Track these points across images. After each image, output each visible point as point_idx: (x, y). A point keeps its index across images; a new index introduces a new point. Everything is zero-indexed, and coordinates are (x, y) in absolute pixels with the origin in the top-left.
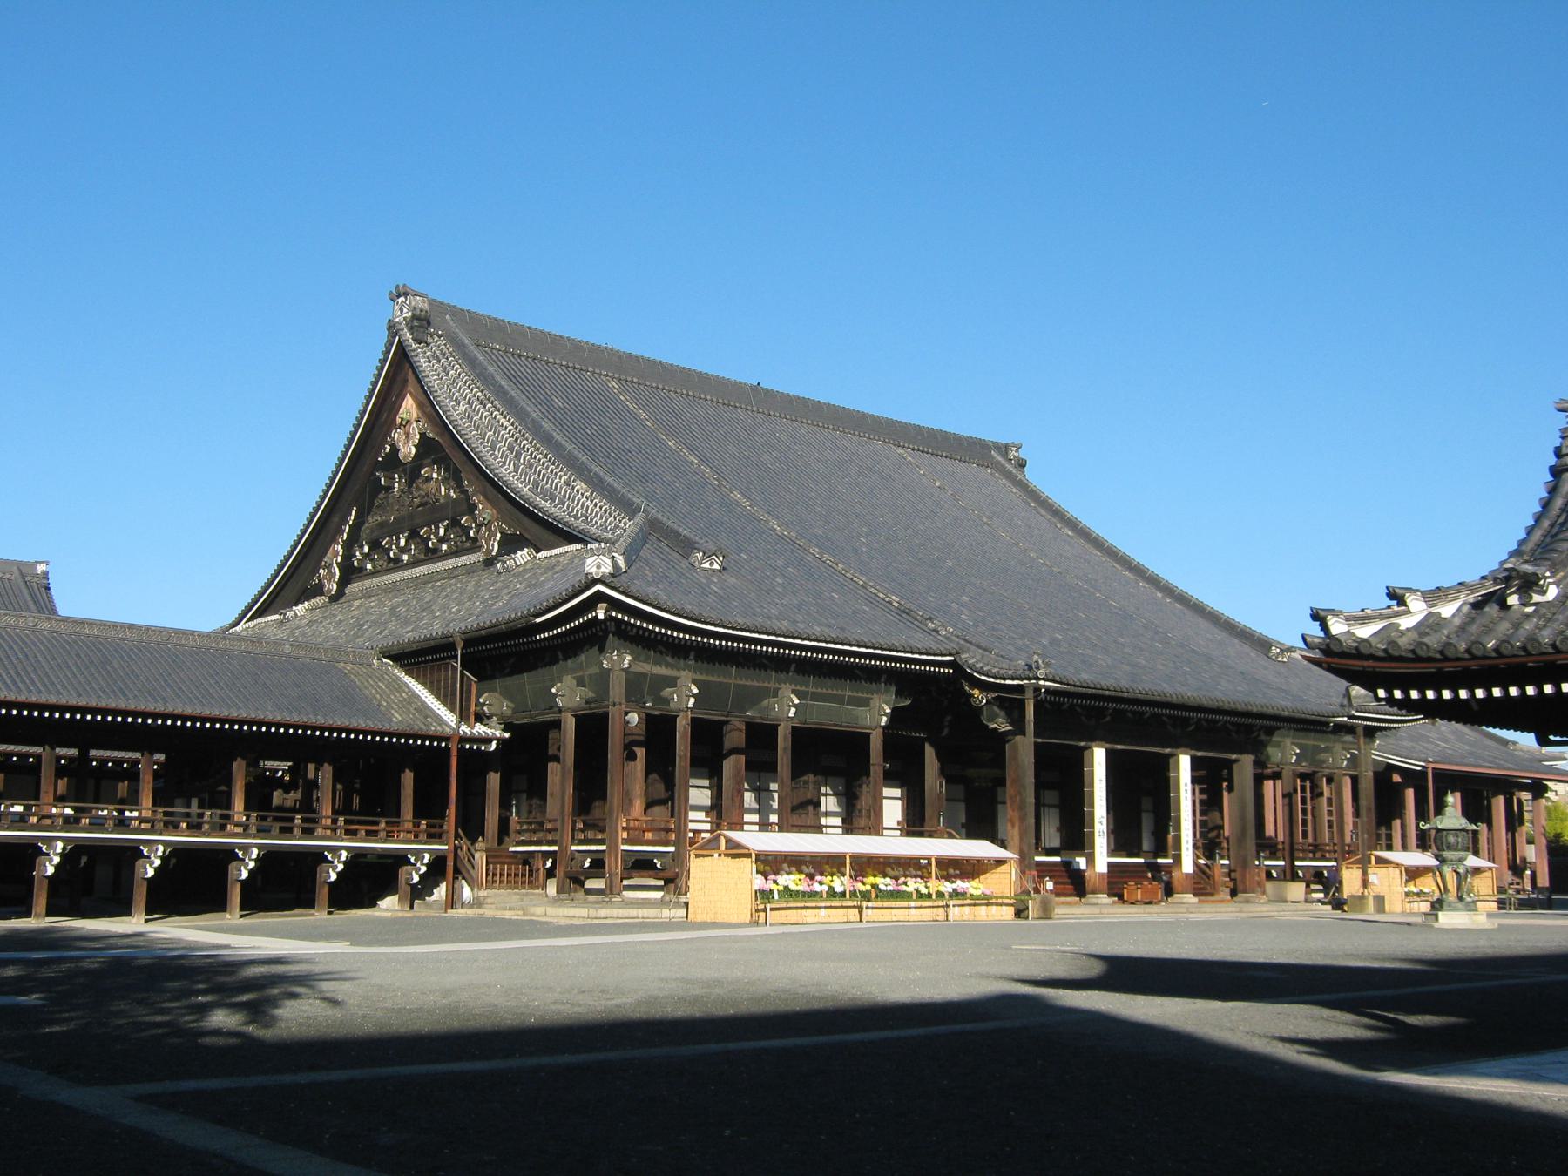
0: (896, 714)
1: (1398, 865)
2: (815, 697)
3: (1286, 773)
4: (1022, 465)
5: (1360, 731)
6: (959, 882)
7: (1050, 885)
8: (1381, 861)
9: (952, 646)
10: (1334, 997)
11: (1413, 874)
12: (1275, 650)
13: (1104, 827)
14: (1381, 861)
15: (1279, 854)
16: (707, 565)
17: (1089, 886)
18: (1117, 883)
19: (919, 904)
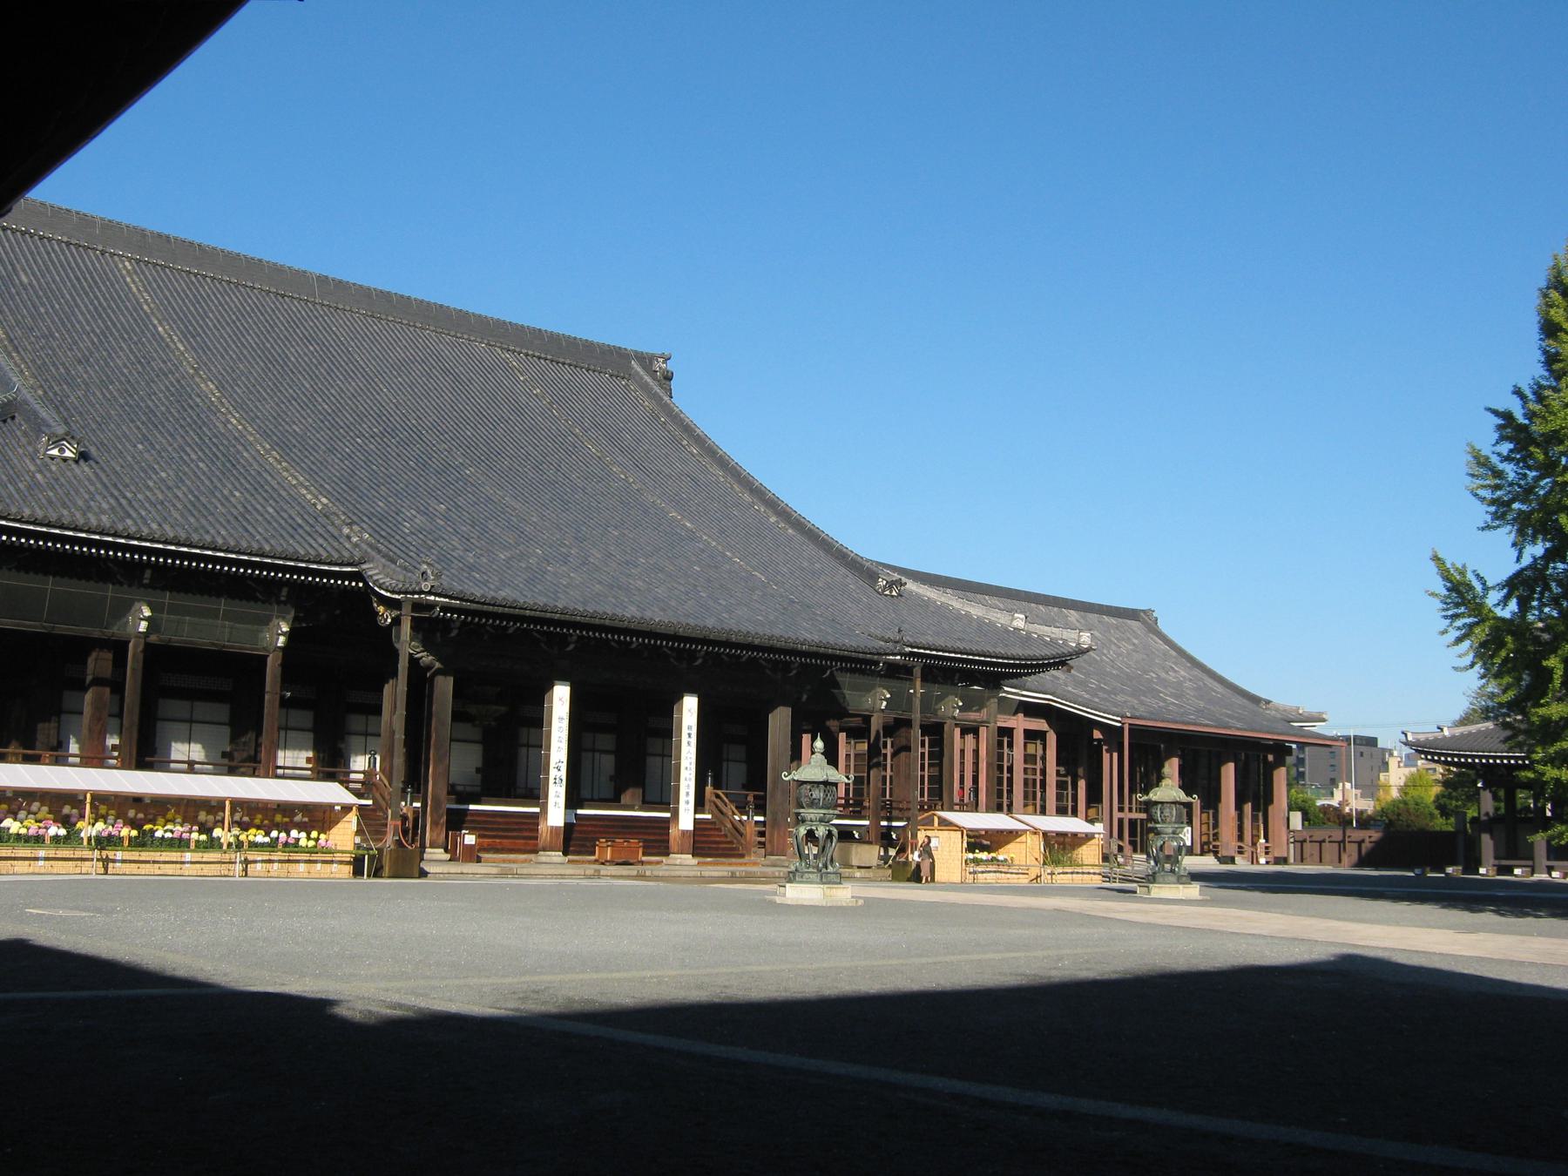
0: (290, 636)
1: (960, 829)
2: (173, 610)
3: (876, 724)
4: (668, 377)
5: (917, 671)
6: (294, 833)
7: (470, 839)
8: (945, 823)
9: (357, 555)
10: (194, 991)
11: (979, 842)
12: (882, 583)
13: (563, 774)
14: (945, 823)
15: (895, 813)
16: (55, 452)
17: (541, 843)
18: (574, 839)
19: (197, 856)
